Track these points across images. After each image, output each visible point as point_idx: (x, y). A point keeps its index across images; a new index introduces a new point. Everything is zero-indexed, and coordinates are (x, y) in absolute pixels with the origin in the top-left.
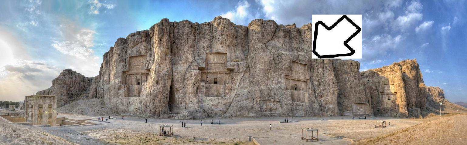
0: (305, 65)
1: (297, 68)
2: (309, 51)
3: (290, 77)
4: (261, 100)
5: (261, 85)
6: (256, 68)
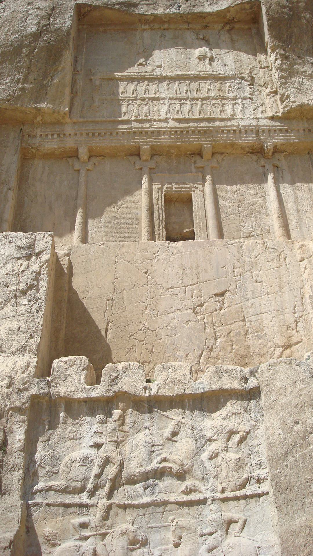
3: (69, 130)
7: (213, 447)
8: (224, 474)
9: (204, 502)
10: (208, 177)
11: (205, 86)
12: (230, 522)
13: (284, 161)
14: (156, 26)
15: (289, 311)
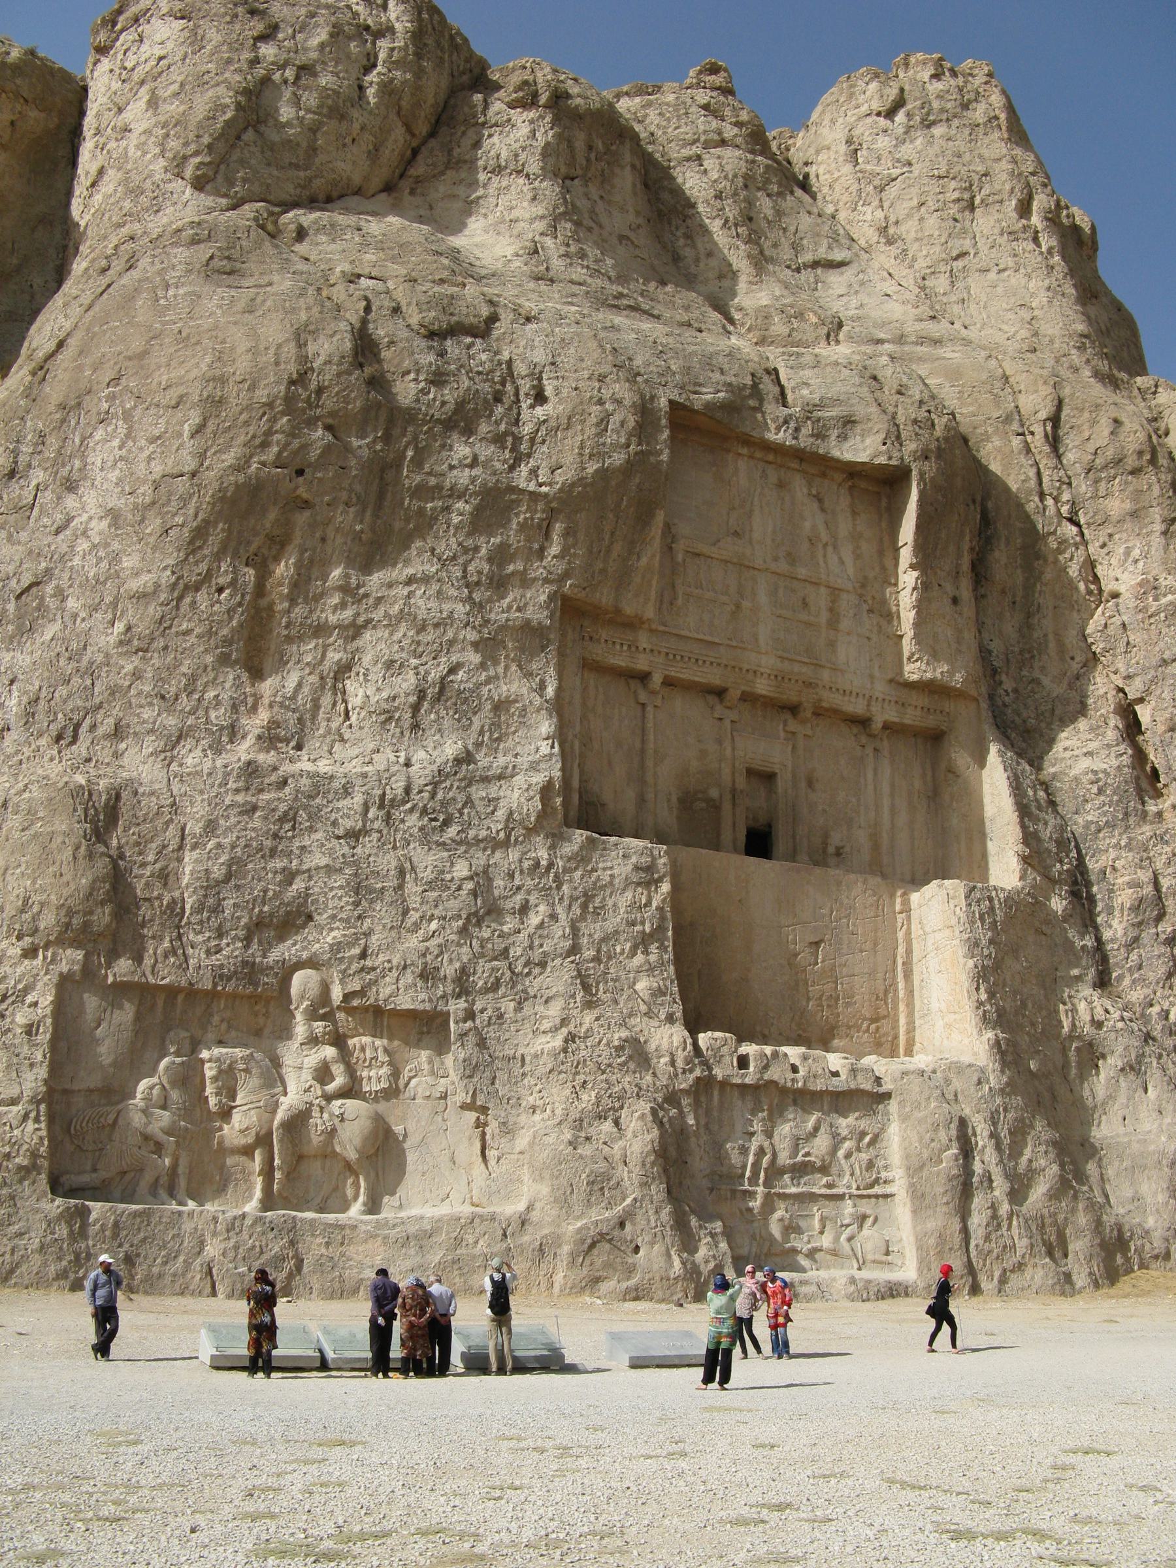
1: (762, 526)
2: (937, 342)
3: (644, 641)
4: (88, 974)
5: (118, 732)
6: (70, 486)
7: (847, 1145)
8: (857, 1172)
9: (841, 1197)
12: (864, 1217)
13: (886, 743)
14: (758, 454)
15: (880, 976)
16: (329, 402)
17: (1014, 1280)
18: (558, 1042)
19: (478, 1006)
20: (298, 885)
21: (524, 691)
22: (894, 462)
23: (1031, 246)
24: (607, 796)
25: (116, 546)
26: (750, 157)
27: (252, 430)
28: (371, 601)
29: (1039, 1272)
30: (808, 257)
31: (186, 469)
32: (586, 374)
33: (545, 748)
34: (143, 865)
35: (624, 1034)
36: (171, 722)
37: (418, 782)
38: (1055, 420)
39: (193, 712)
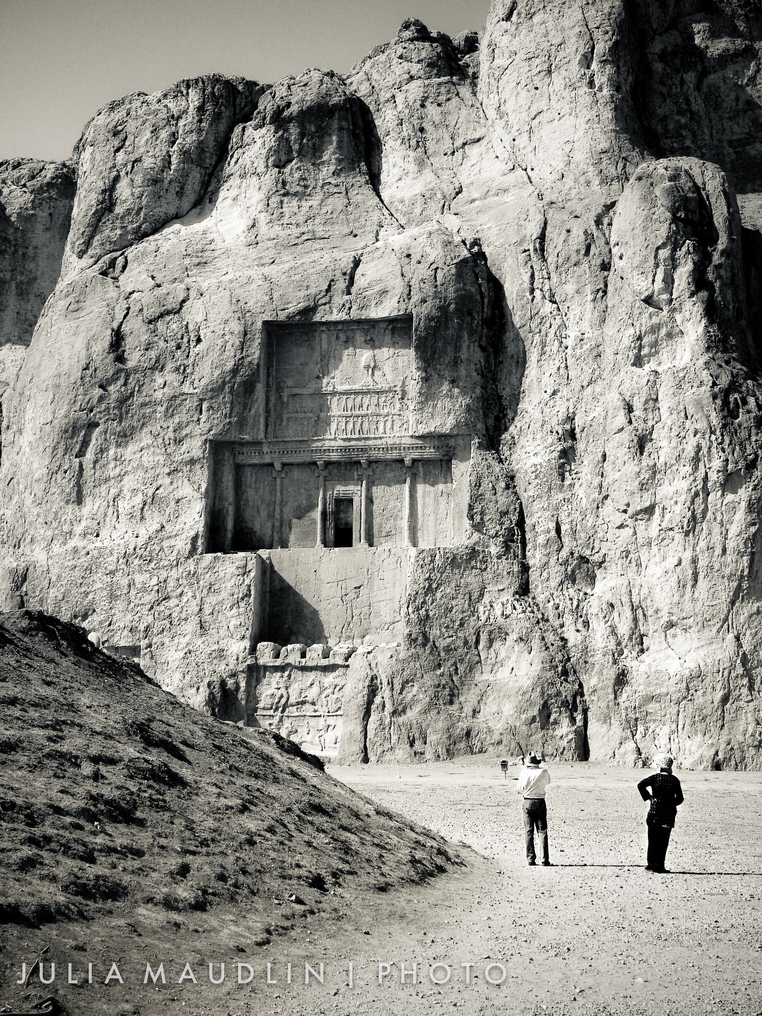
0: (407, 319)
3: (265, 449)
7: (329, 691)
10: (364, 482)
11: (366, 400)
13: (421, 469)
16: (100, 374)
17: (388, 756)
18: (182, 654)
19: (154, 641)
20: (90, 597)
21: (191, 491)
22: (401, 313)
23: (586, 89)
24: (257, 527)
25: (32, 459)
26: (427, 82)
27: (70, 397)
28: (127, 462)
29: (402, 751)
30: (459, 142)
31: (49, 421)
32: (219, 321)
33: (197, 518)
34: (34, 598)
35: (216, 647)
36: (49, 533)
37: (139, 545)
38: (542, 237)
39: (57, 528)
